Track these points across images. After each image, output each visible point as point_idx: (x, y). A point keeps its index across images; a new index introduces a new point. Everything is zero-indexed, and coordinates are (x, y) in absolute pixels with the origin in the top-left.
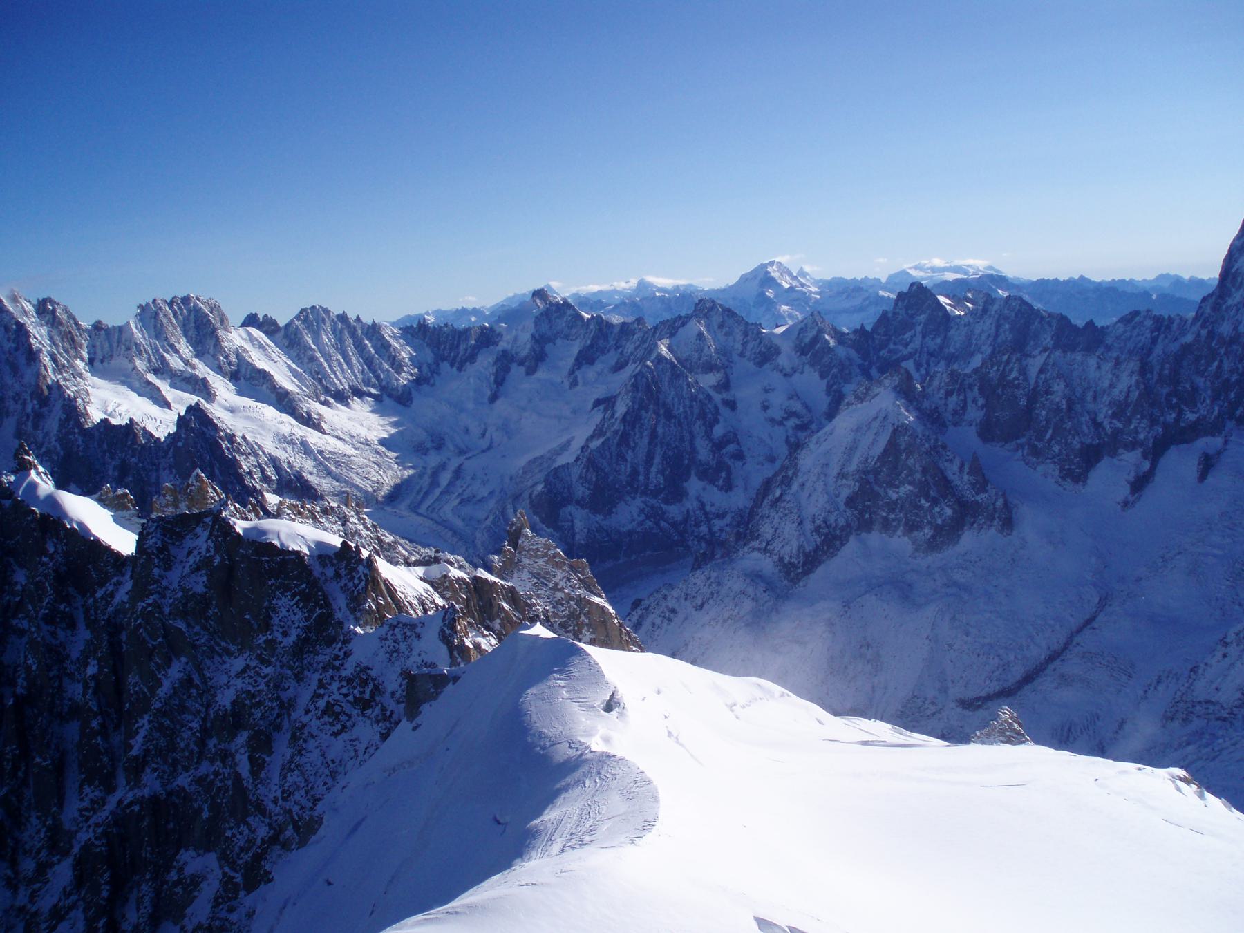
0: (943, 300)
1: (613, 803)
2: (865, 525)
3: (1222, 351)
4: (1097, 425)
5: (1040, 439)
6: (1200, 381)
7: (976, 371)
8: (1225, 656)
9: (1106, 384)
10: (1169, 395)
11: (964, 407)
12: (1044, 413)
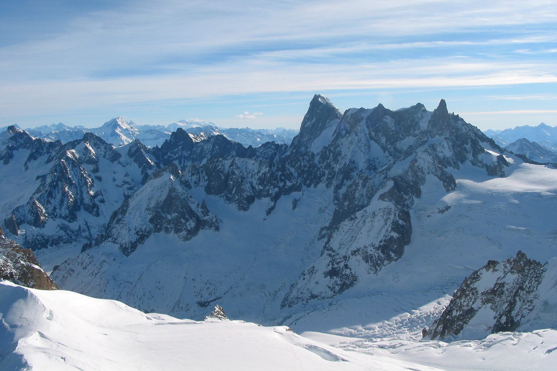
0: (191, 136)
1: (31, 303)
2: (158, 230)
3: (301, 158)
4: (253, 188)
5: (230, 193)
6: (292, 170)
7: (204, 165)
8: (304, 279)
9: (256, 171)
10: (281, 176)
11: (199, 180)
12: (232, 183)
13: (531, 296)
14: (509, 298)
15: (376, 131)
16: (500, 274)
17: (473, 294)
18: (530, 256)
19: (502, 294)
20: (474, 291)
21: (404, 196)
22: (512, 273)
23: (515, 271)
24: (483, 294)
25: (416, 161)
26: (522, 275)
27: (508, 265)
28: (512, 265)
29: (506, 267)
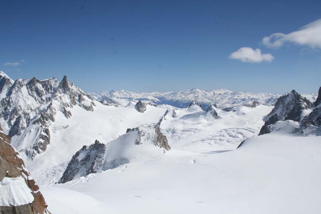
13: (101, 159)
14: (92, 162)
15: (32, 90)
16: (88, 151)
17: (77, 162)
18: (101, 142)
19: (89, 160)
20: (77, 161)
21: (46, 121)
22: (93, 150)
23: (95, 149)
24: (81, 161)
25: (51, 104)
26: (98, 150)
27: (92, 147)
28: (93, 147)
29: (91, 148)
